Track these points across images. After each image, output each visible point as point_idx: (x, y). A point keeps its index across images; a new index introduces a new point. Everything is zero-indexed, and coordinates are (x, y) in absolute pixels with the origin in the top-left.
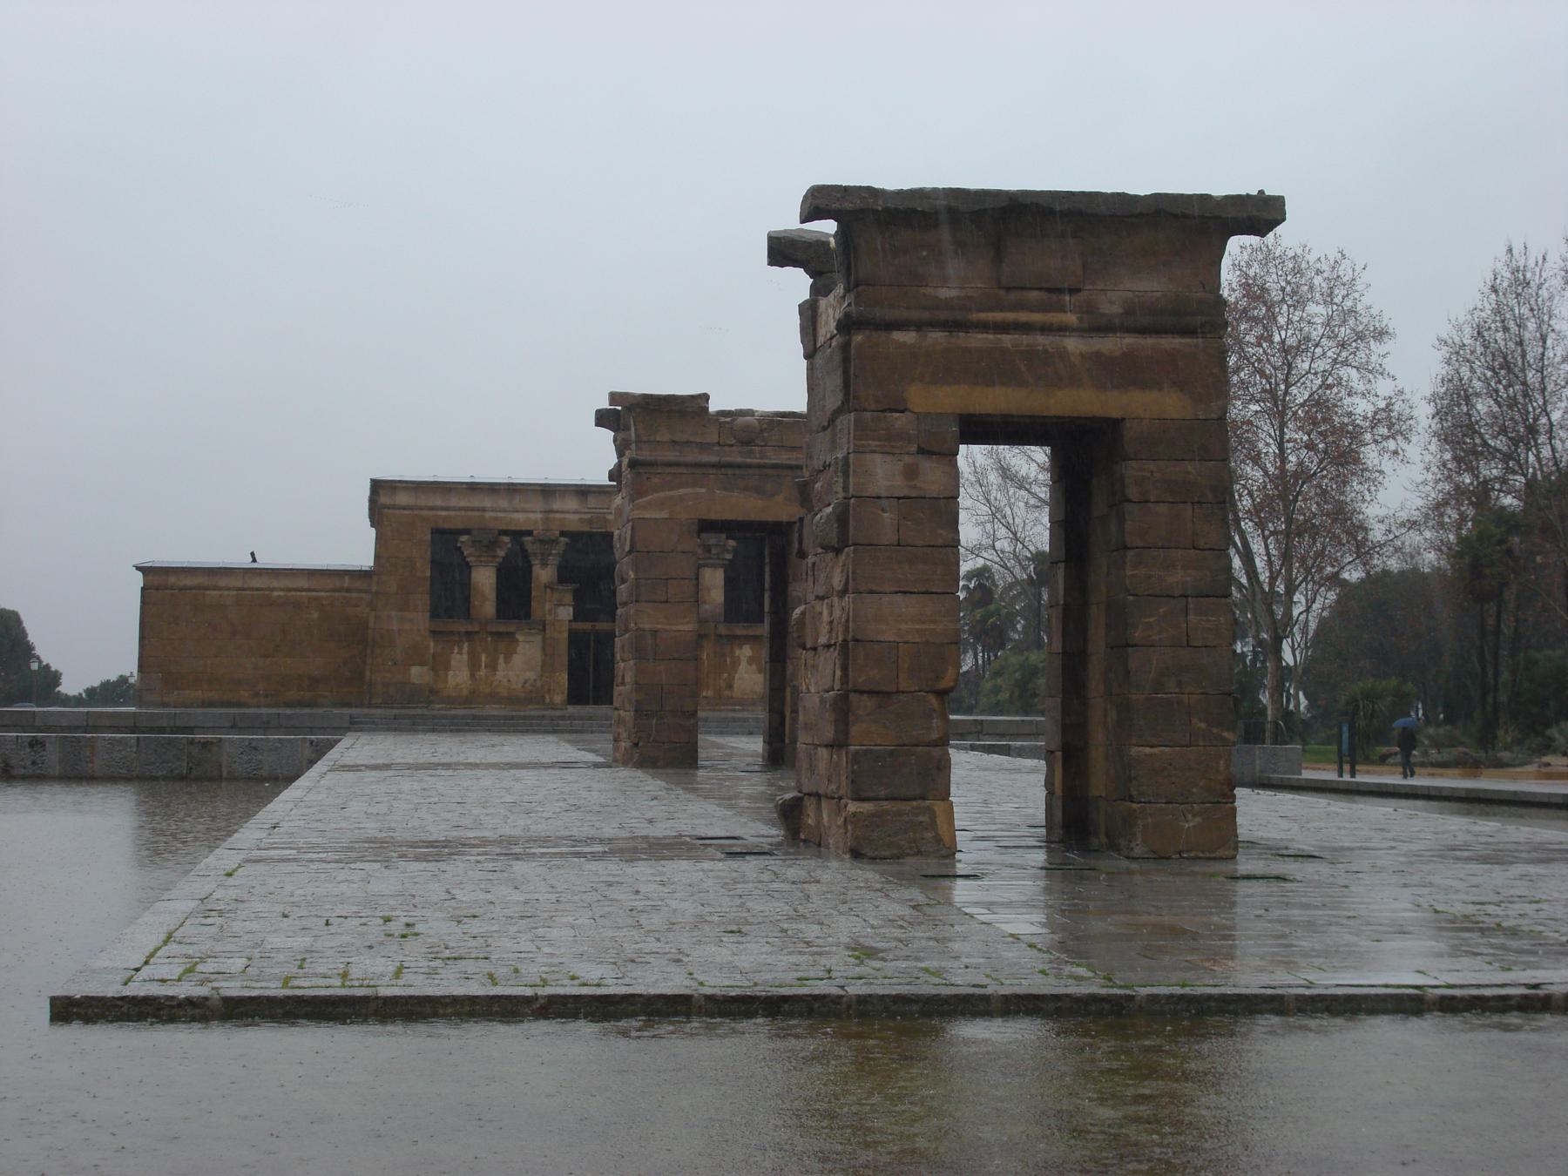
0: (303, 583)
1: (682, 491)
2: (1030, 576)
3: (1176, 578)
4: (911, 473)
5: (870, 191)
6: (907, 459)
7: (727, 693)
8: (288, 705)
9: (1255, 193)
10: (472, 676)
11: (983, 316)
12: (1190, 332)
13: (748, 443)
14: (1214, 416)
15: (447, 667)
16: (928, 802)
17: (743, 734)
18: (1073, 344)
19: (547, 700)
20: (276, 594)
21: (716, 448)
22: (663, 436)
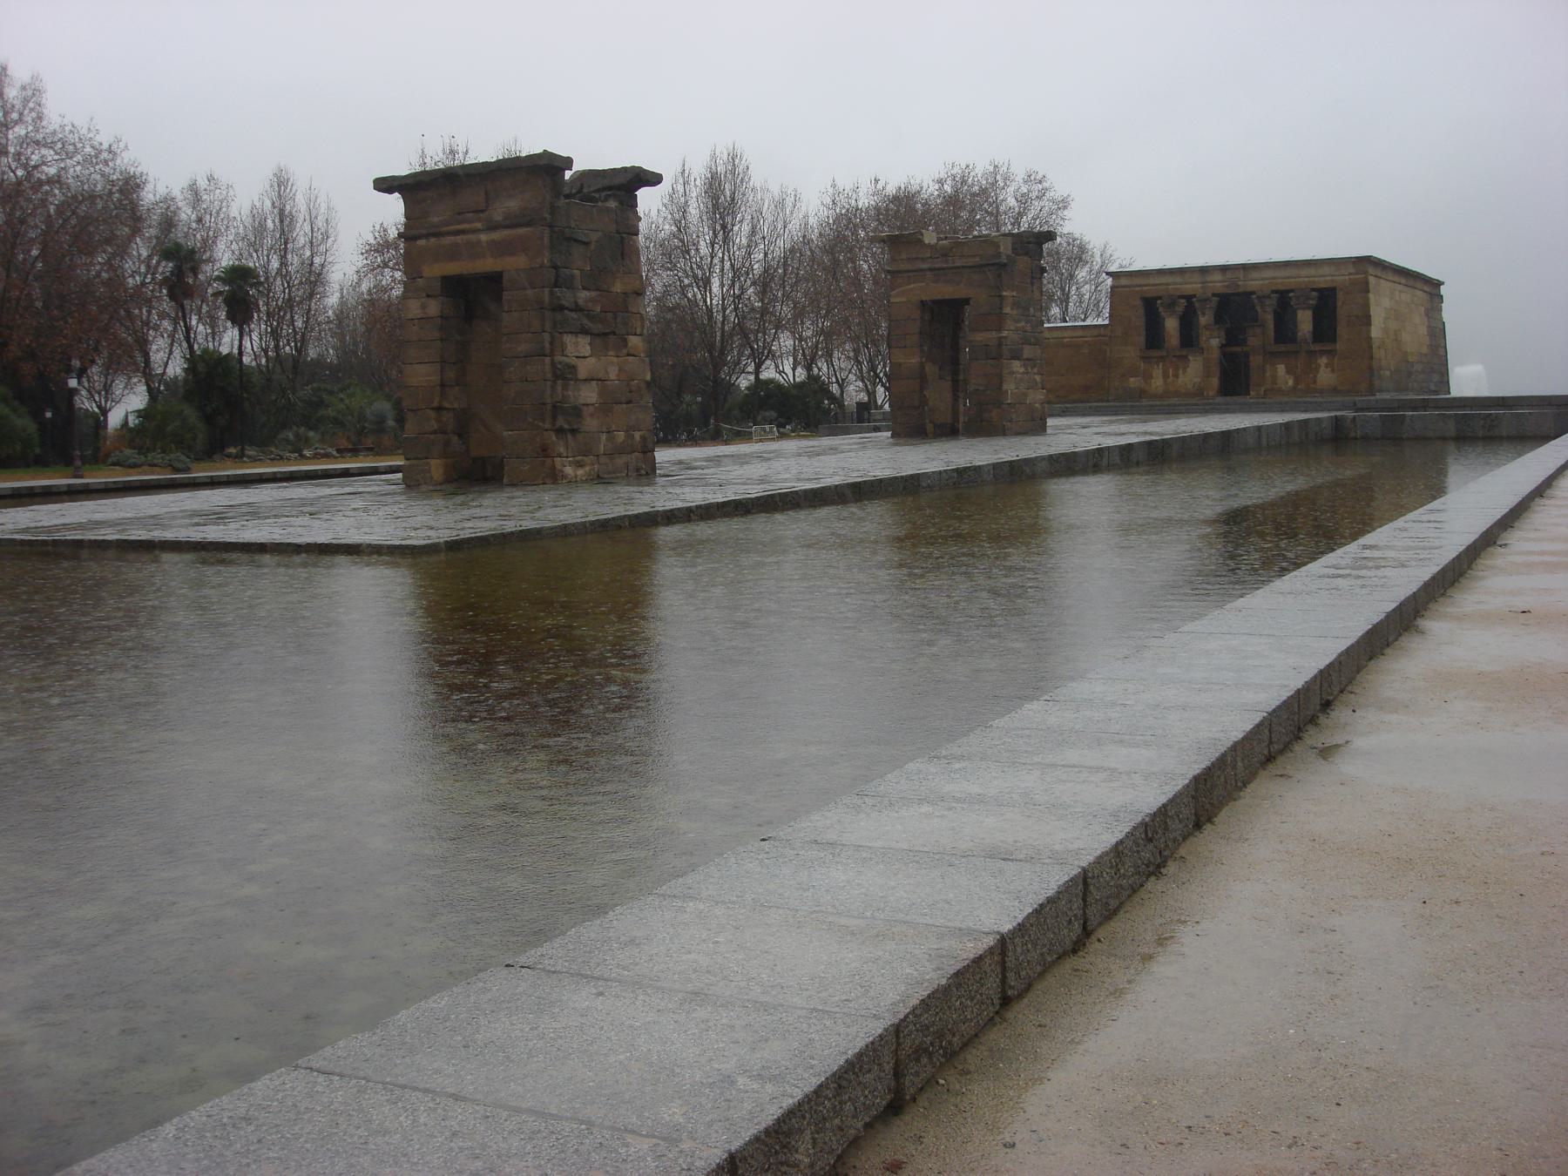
0: (1080, 333)
1: (912, 286)
2: (259, 365)
3: (523, 348)
4: (423, 307)
5: (393, 178)
6: (423, 300)
7: (1313, 386)
8: (1074, 402)
9: (542, 151)
10: (1165, 381)
11: (445, 229)
12: (528, 224)
13: (945, 255)
14: (538, 265)
15: (1151, 377)
16: (428, 460)
17: (1278, 411)
18: (484, 237)
19: (1205, 394)
20: (1065, 340)
21: (930, 260)
22: (904, 256)
